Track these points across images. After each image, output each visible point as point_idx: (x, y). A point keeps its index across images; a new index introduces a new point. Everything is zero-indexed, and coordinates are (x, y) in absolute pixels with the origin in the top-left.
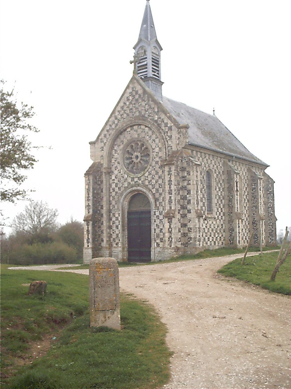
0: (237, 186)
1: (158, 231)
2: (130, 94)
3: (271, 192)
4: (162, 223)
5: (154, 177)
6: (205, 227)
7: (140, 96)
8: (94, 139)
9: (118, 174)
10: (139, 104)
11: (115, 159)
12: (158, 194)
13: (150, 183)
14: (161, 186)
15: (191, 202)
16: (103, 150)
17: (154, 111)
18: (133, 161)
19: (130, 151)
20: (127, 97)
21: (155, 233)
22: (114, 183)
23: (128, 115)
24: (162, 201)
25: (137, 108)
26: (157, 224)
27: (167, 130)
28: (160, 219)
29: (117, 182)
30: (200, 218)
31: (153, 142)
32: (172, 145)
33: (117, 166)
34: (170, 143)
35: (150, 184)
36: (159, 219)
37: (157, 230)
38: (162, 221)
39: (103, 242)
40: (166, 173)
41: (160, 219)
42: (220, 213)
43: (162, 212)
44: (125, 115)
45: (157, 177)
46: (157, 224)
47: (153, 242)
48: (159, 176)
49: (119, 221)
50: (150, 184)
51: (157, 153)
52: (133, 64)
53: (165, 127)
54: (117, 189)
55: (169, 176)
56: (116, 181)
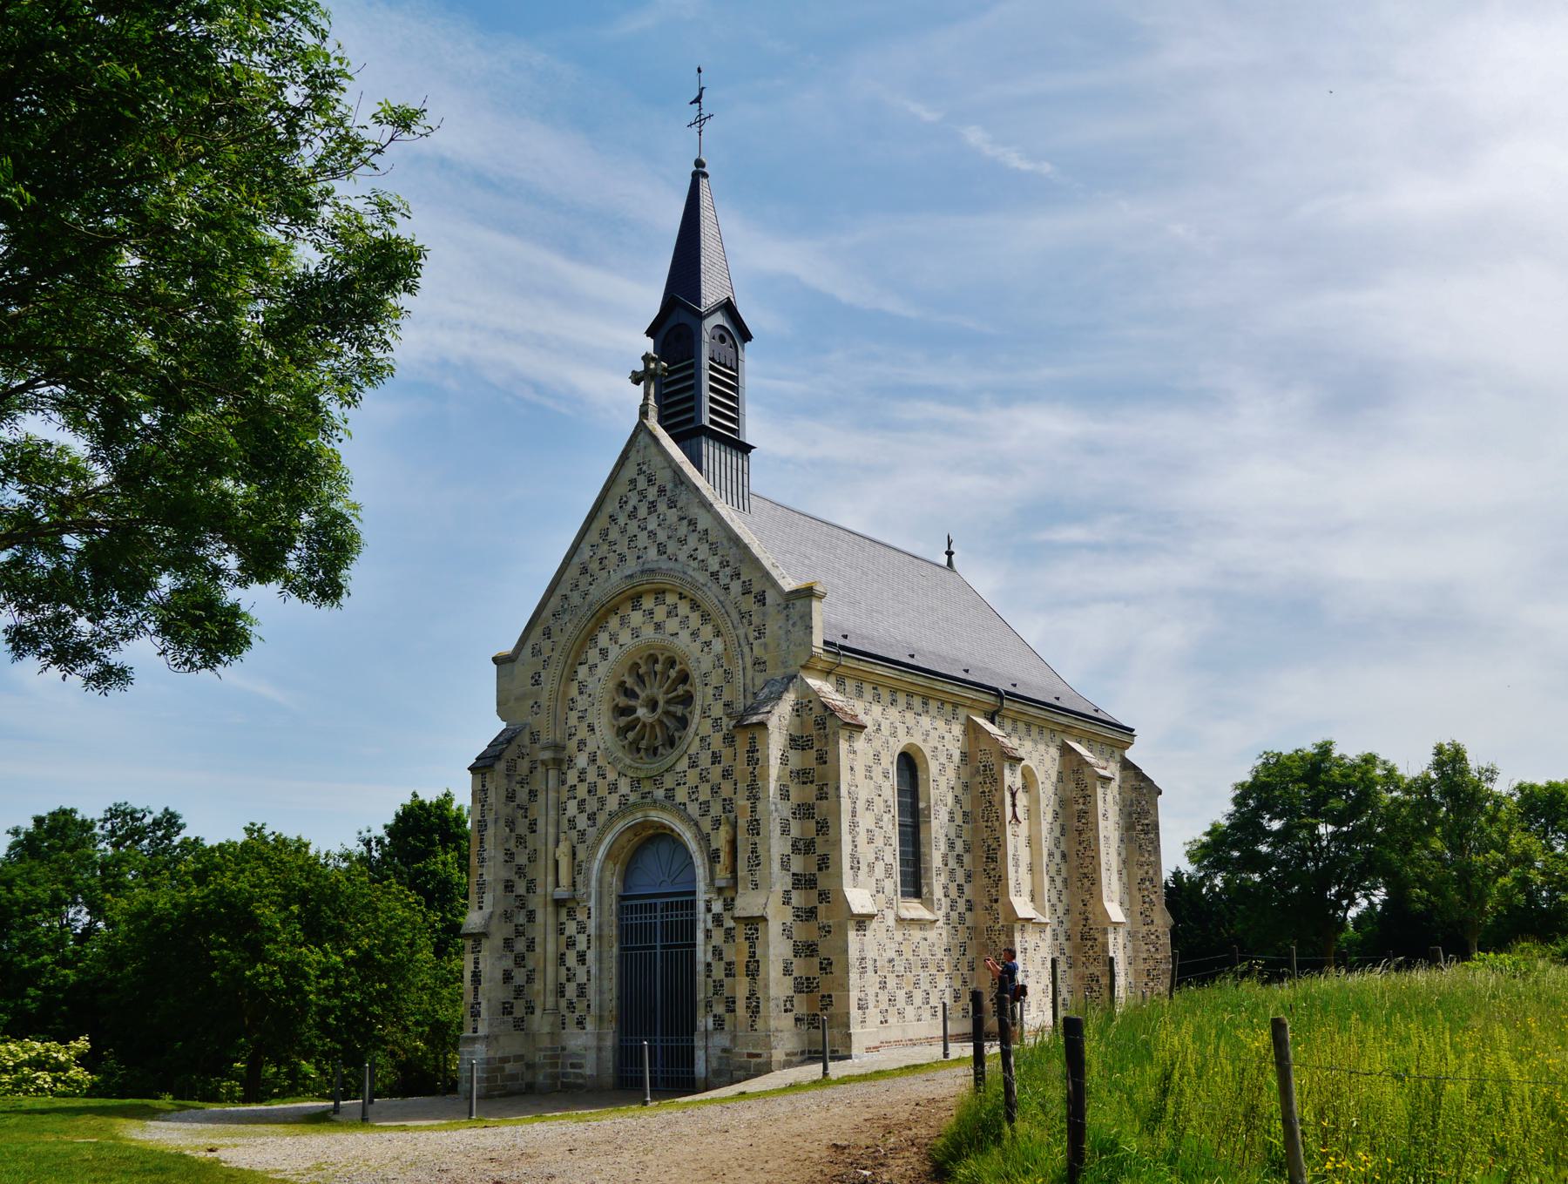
0: (1014, 805)
1: (718, 972)
2: (631, 487)
3: (1147, 825)
6: (893, 955)
7: (662, 491)
8: (508, 647)
11: (580, 714)
13: (693, 797)
18: (638, 719)
19: (628, 685)
21: (708, 976)
22: (575, 798)
25: (652, 534)
30: (864, 922)
32: (765, 659)
34: (758, 651)
39: (532, 1013)
40: (743, 756)
42: (954, 902)
45: (716, 771)
47: (701, 1012)
49: (589, 936)
52: (642, 383)
54: (582, 822)
55: (751, 770)
56: (582, 791)
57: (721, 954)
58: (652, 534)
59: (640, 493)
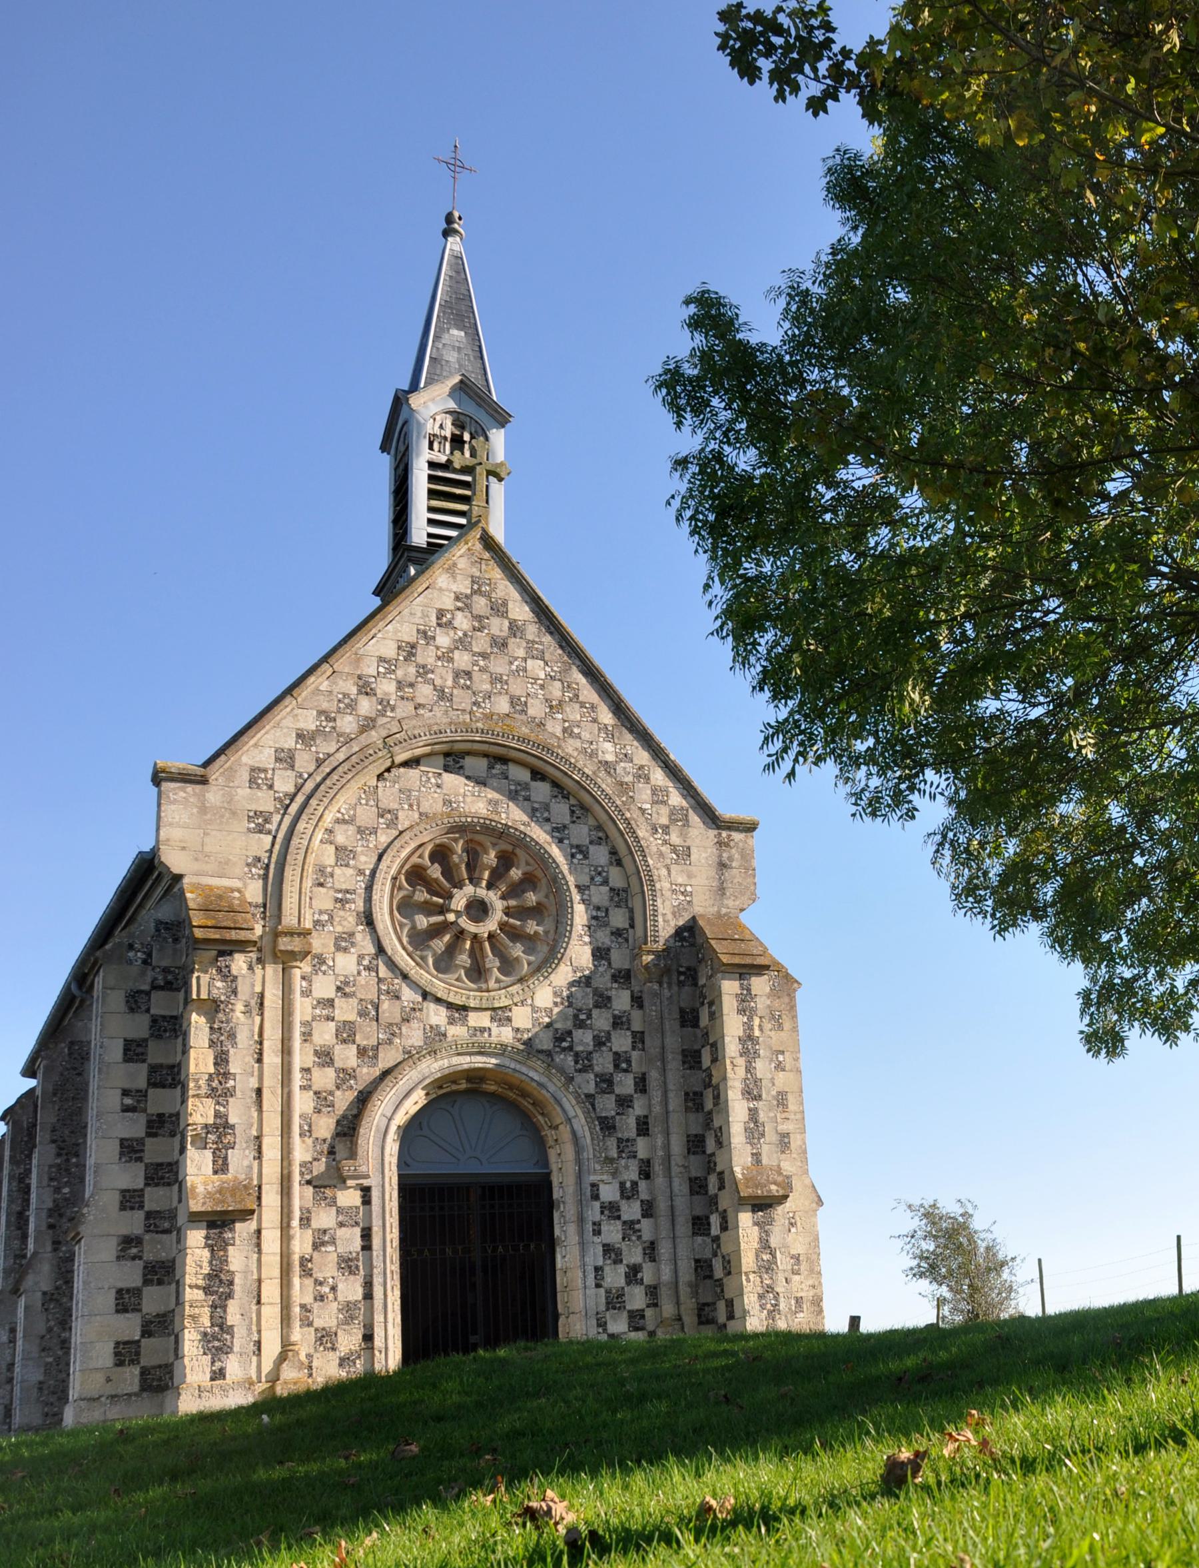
2: (460, 604)
4: (639, 1237)
5: (589, 1016)
9: (359, 973)
10: (511, 663)
12: (613, 1098)
14: (624, 1065)
15: (793, 1146)
16: (260, 830)
17: (595, 721)
20: (441, 614)
21: (598, 1286)
23: (441, 694)
24: (633, 1133)
26: (604, 1245)
27: (664, 820)
28: (625, 1217)
29: (352, 1016)
31: (579, 856)
33: (352, 935)
35: (564, 1049)
36: (619, 1217)
37: (607, 1269)
38: (637, 1227)
41: (625, 1217)
43: (635, 1184)
44: (425, 692)
45: (601, 1020)
46: (604, 1245)
48: (615, 1017)
50: (564, 1049)
51: (598, 908)
53: (654, 803)
57: (618, 1253)
58: (496, 679)
59: (479, 618)
